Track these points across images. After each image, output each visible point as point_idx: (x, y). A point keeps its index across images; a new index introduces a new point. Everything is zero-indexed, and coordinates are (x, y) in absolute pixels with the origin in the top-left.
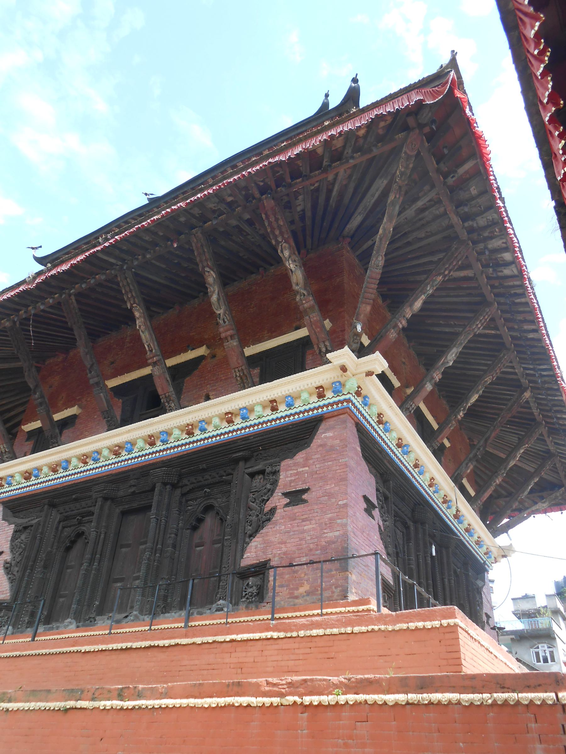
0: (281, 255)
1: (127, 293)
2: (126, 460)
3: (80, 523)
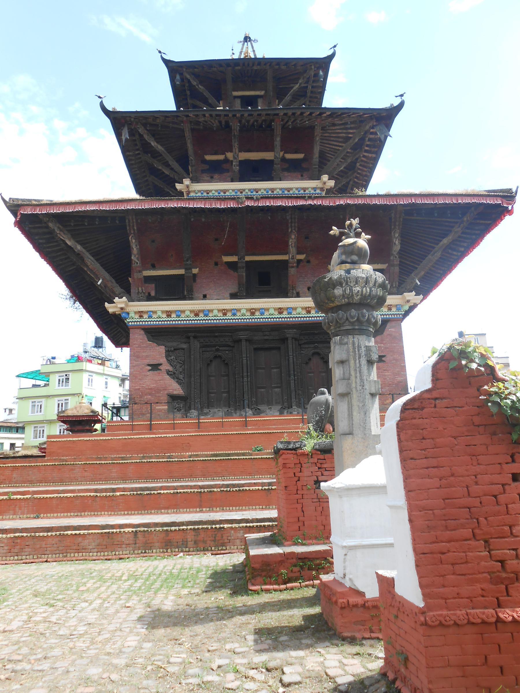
0: (393, 234)
1: (291, 222)
2: (258, 318)
3: (217, 350)
